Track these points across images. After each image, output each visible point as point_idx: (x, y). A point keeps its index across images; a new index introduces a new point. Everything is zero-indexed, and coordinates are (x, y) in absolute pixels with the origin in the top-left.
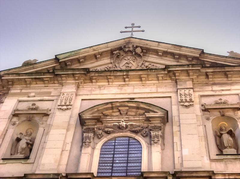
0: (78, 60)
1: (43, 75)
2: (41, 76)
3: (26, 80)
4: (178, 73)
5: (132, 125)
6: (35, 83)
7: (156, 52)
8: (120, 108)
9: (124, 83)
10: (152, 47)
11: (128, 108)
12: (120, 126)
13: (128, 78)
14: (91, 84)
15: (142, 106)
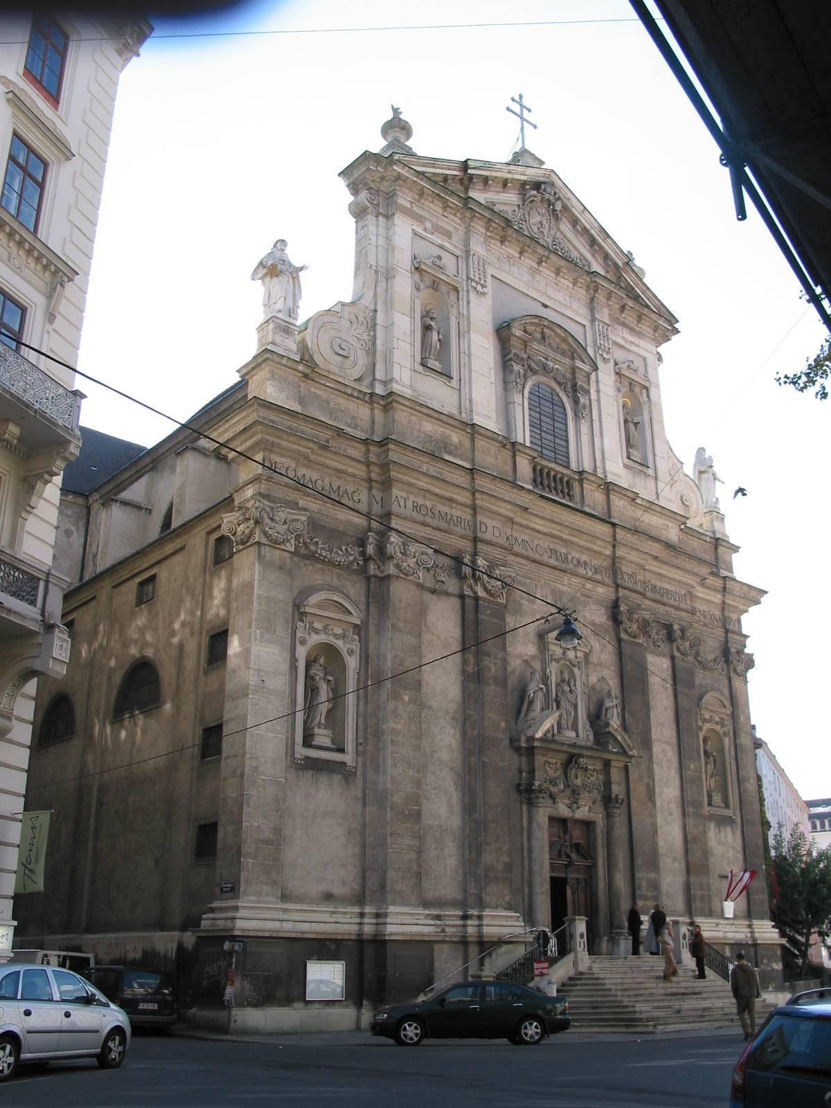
0: (486, 180)
1: (450, 196)
2: (446, 194)
3: (425, 189)
4: (601, 289)
5: (557, 369)
6: (430, 199)
7: (575, 222)
8: (545, 330)
9: (536, 266)
10: (573, 209)
11: (553, 334)
12: (547, 368)
13: (546, 262)
14: (499, 244)
15: (570, 340)
